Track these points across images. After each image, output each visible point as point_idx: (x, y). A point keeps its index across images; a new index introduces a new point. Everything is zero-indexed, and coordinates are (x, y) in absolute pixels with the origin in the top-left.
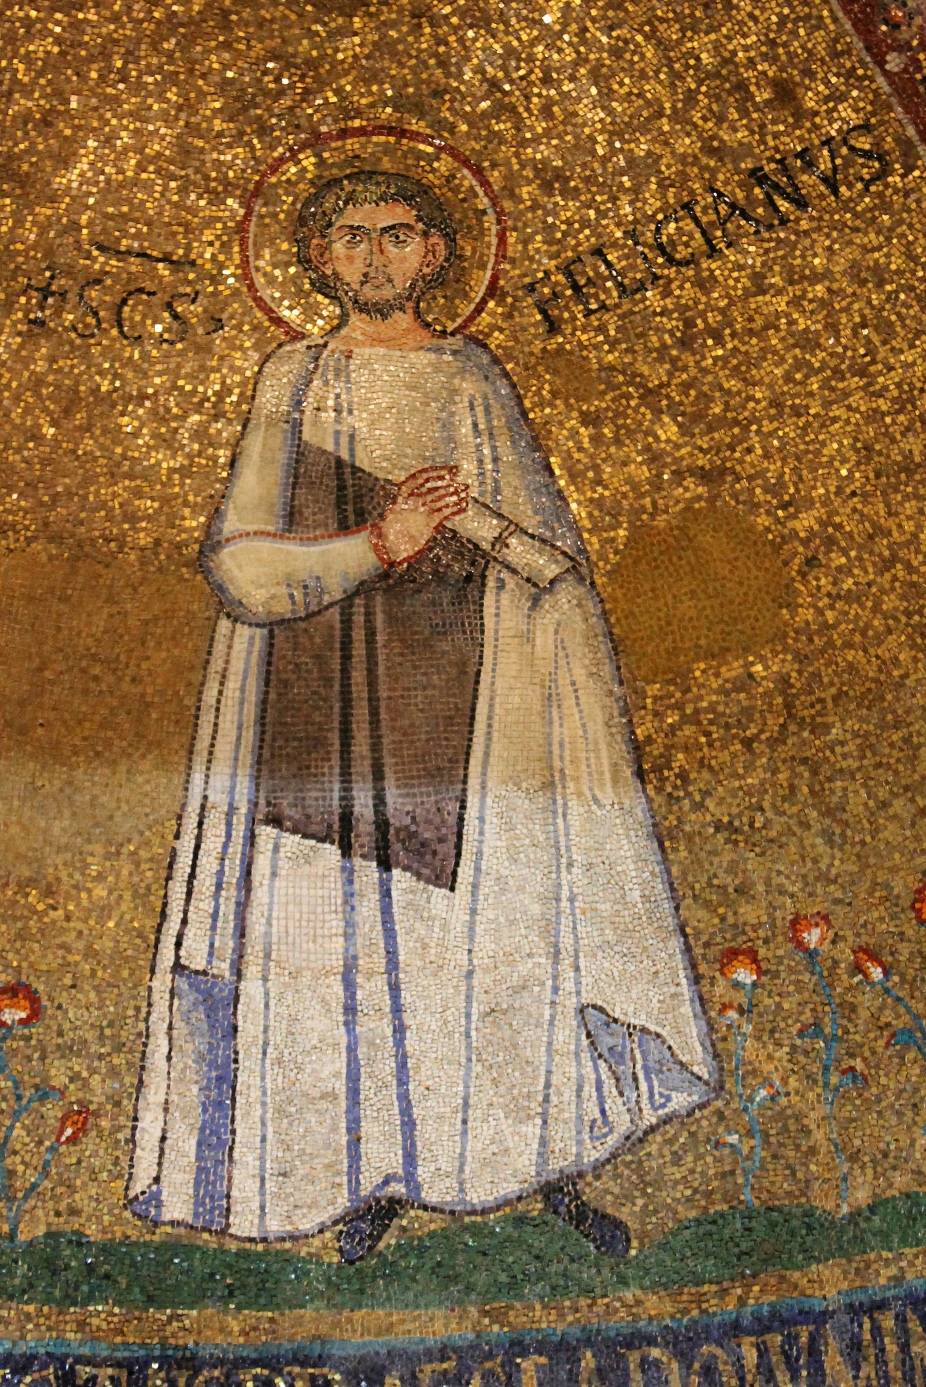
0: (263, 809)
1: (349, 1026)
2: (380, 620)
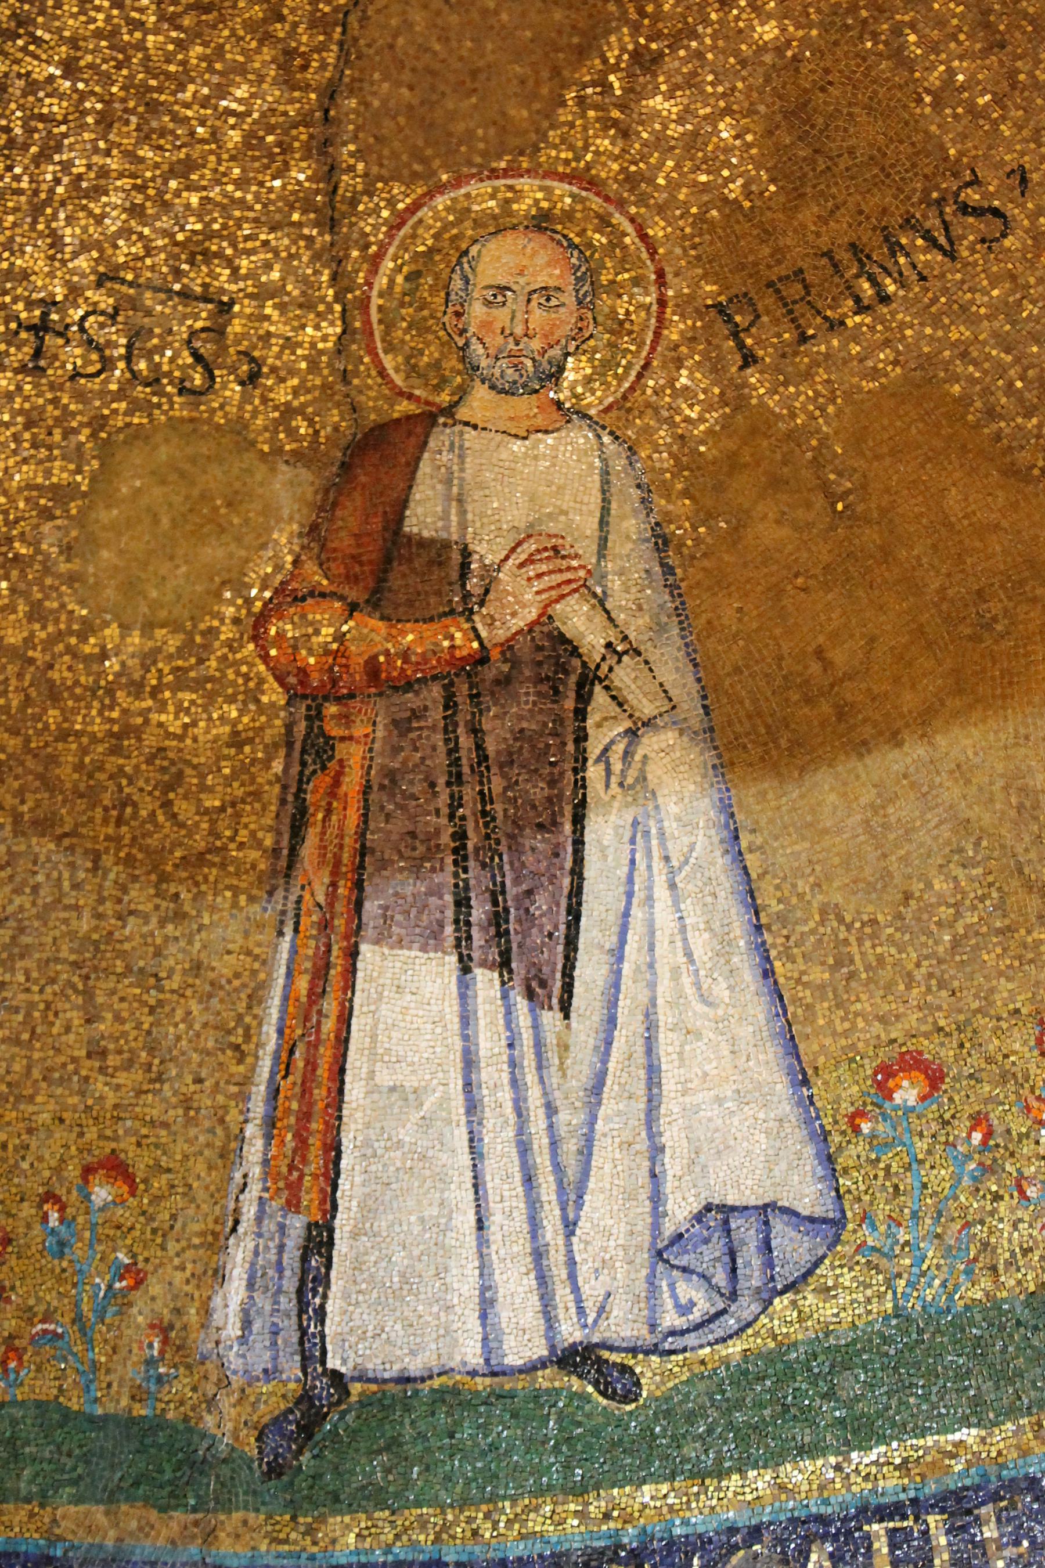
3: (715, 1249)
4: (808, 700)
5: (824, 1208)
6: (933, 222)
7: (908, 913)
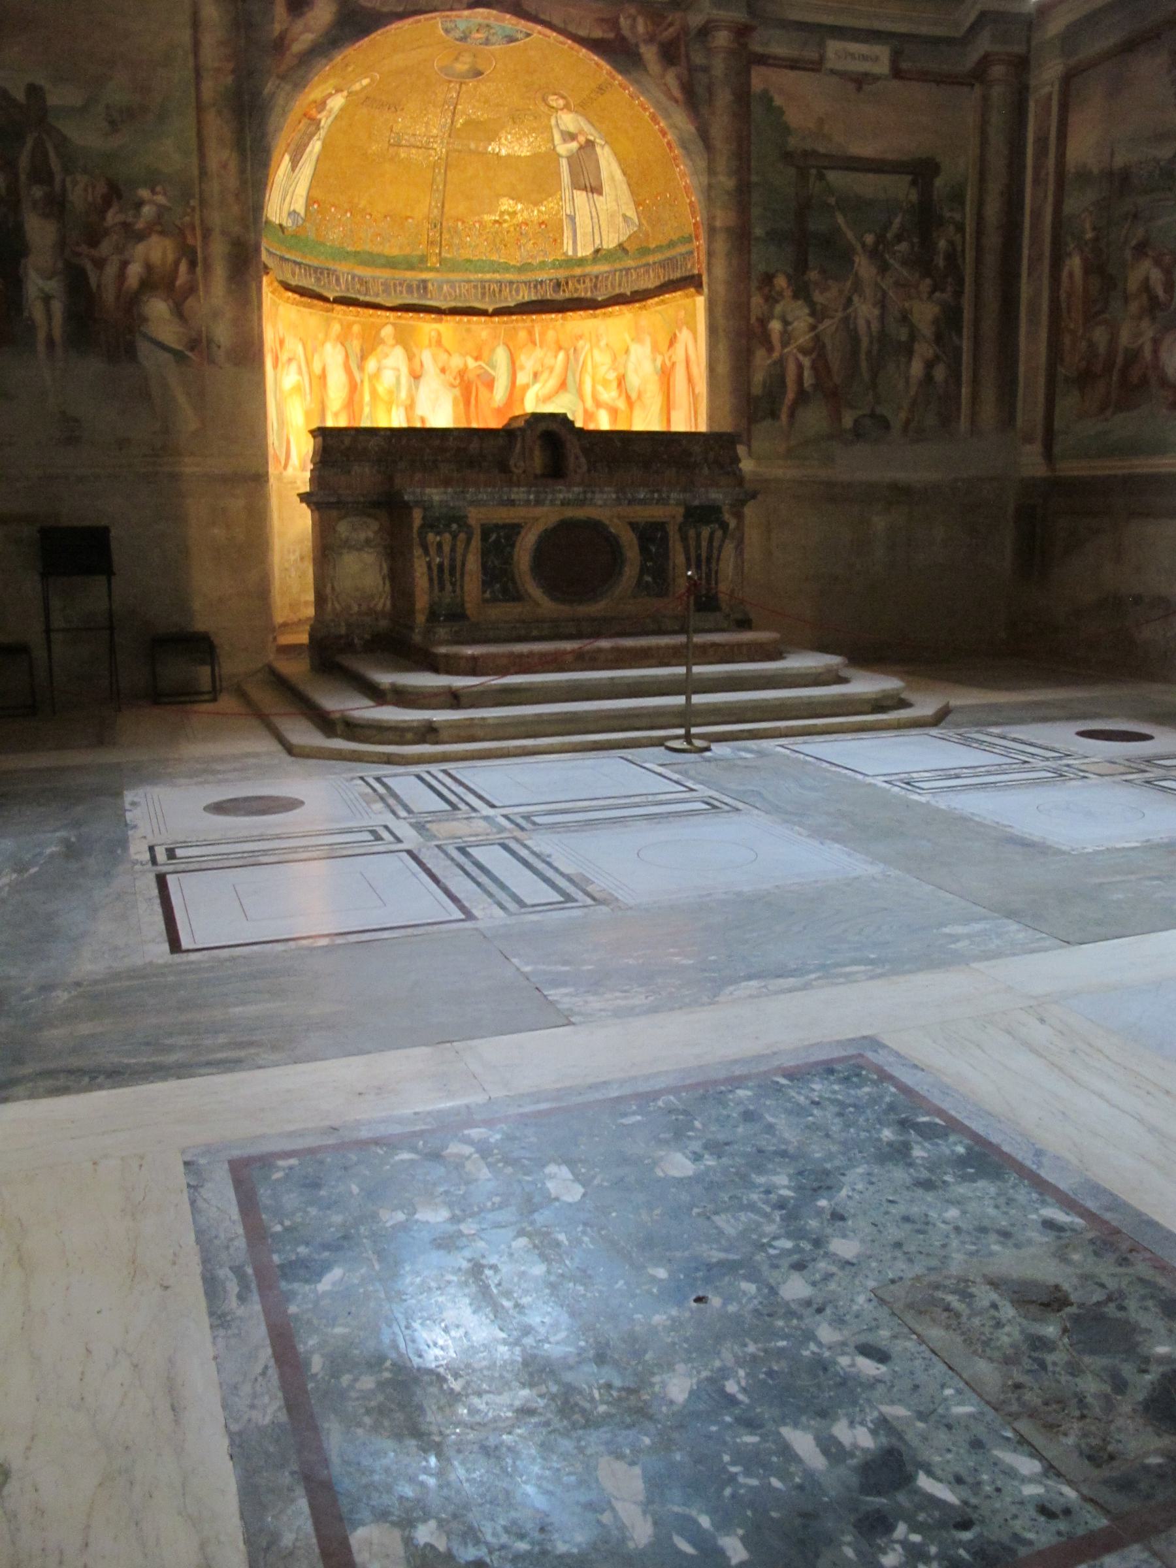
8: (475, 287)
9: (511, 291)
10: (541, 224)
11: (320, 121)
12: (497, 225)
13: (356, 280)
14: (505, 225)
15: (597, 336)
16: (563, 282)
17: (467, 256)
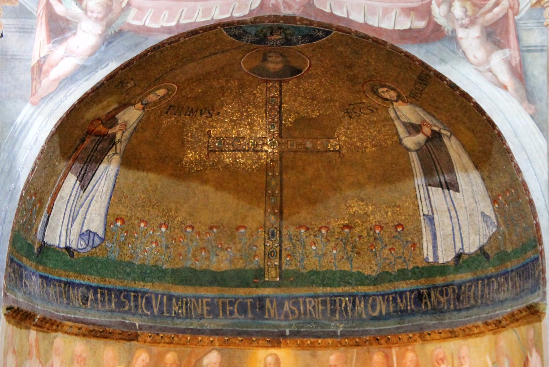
0: (427, 184)
1: (451, 220)
2: (432, 147)
3: (87, 237)
4: (135, 159)
5: (103, 237)
6: (203, 111)
7: (132, 197)
8: (324, 303)
9: (366, 307)
10: (396, 227)
11: (114, 135)
12: (347, 230)
13: (174, 301)
14: (357, 230)
15: (459, 358)
16: (425, 292)
17: (314, 268)
